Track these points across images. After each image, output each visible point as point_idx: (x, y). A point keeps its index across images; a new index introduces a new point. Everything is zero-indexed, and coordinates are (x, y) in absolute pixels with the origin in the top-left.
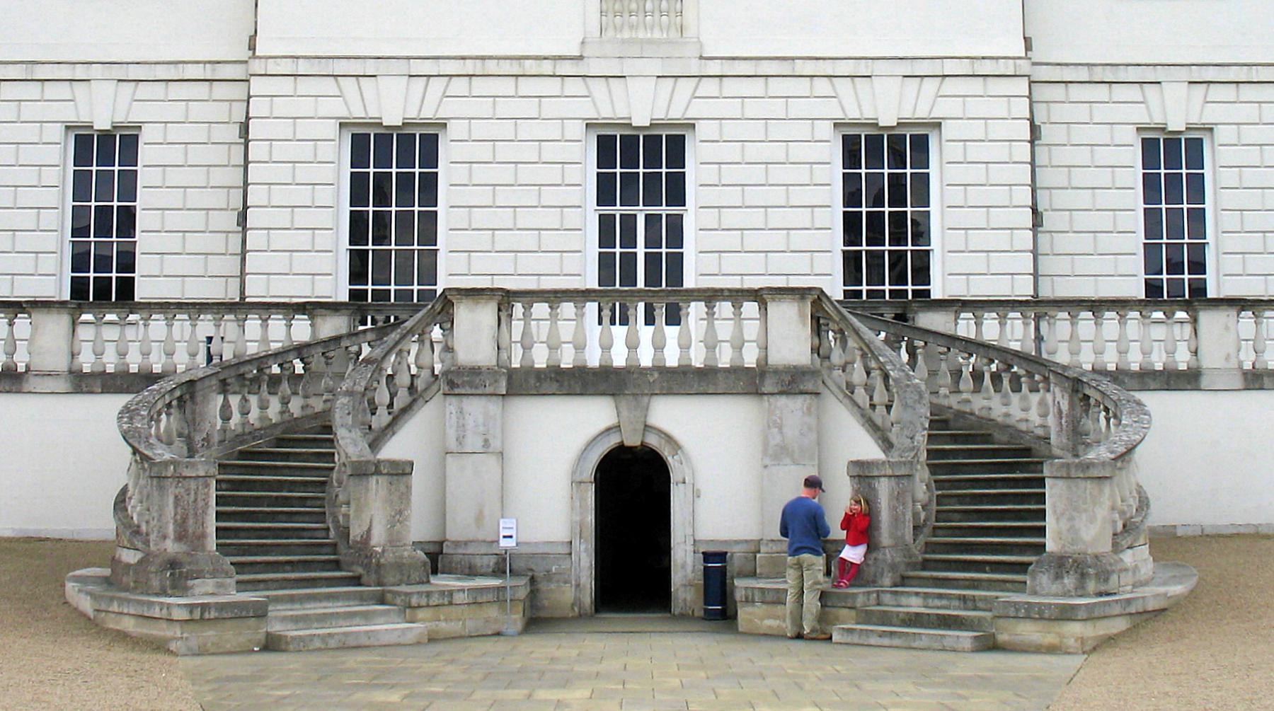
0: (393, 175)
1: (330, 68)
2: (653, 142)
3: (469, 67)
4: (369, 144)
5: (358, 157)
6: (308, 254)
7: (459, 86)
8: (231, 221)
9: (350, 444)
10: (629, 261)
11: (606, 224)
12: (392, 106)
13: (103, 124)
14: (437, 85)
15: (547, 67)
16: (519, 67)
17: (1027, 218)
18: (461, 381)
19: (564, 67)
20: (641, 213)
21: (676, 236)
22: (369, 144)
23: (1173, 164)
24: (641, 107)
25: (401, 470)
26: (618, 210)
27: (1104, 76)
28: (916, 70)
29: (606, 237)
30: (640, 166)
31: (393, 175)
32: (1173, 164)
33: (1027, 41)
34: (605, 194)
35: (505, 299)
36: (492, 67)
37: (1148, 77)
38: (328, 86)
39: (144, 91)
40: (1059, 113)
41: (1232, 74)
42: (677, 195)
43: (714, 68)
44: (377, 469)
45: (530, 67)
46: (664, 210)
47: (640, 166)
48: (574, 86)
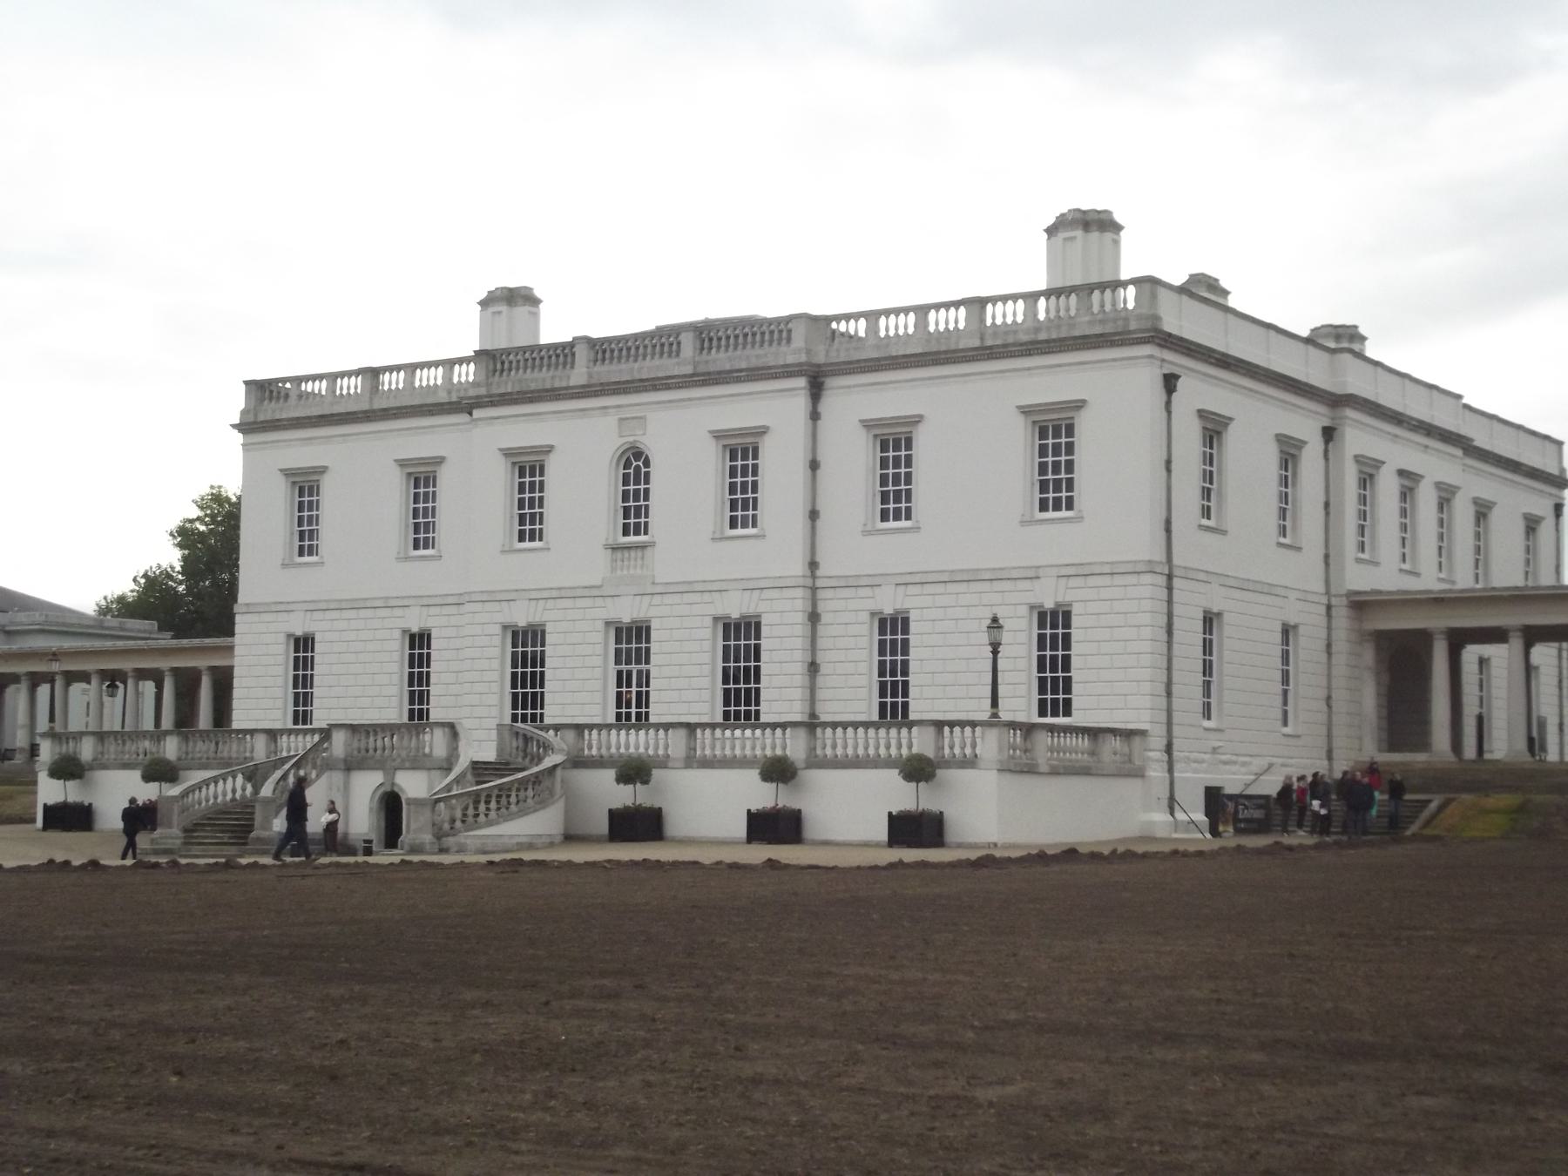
1: (492, 598)
3: (555, 594)
7: (550, 603)
11: (620, 673)
12: (522, 617)
14: (541, 603)
15: (586, 592)
19: (593, 592)
20: (634, 667)
24: (627, 612)
26: (624, 667)
27: (851, 583)
28: (751, 587)
33: (813, 565)
34: (618, 662)
36: (563, 593)
37: (874, 583)
38: (496, 606)
39: (433, 610)
40: (831, 605)
41: (917, 579)
43: (659, 589)
45: (579, 593)
46: (643, 666)
48: (599, 601)
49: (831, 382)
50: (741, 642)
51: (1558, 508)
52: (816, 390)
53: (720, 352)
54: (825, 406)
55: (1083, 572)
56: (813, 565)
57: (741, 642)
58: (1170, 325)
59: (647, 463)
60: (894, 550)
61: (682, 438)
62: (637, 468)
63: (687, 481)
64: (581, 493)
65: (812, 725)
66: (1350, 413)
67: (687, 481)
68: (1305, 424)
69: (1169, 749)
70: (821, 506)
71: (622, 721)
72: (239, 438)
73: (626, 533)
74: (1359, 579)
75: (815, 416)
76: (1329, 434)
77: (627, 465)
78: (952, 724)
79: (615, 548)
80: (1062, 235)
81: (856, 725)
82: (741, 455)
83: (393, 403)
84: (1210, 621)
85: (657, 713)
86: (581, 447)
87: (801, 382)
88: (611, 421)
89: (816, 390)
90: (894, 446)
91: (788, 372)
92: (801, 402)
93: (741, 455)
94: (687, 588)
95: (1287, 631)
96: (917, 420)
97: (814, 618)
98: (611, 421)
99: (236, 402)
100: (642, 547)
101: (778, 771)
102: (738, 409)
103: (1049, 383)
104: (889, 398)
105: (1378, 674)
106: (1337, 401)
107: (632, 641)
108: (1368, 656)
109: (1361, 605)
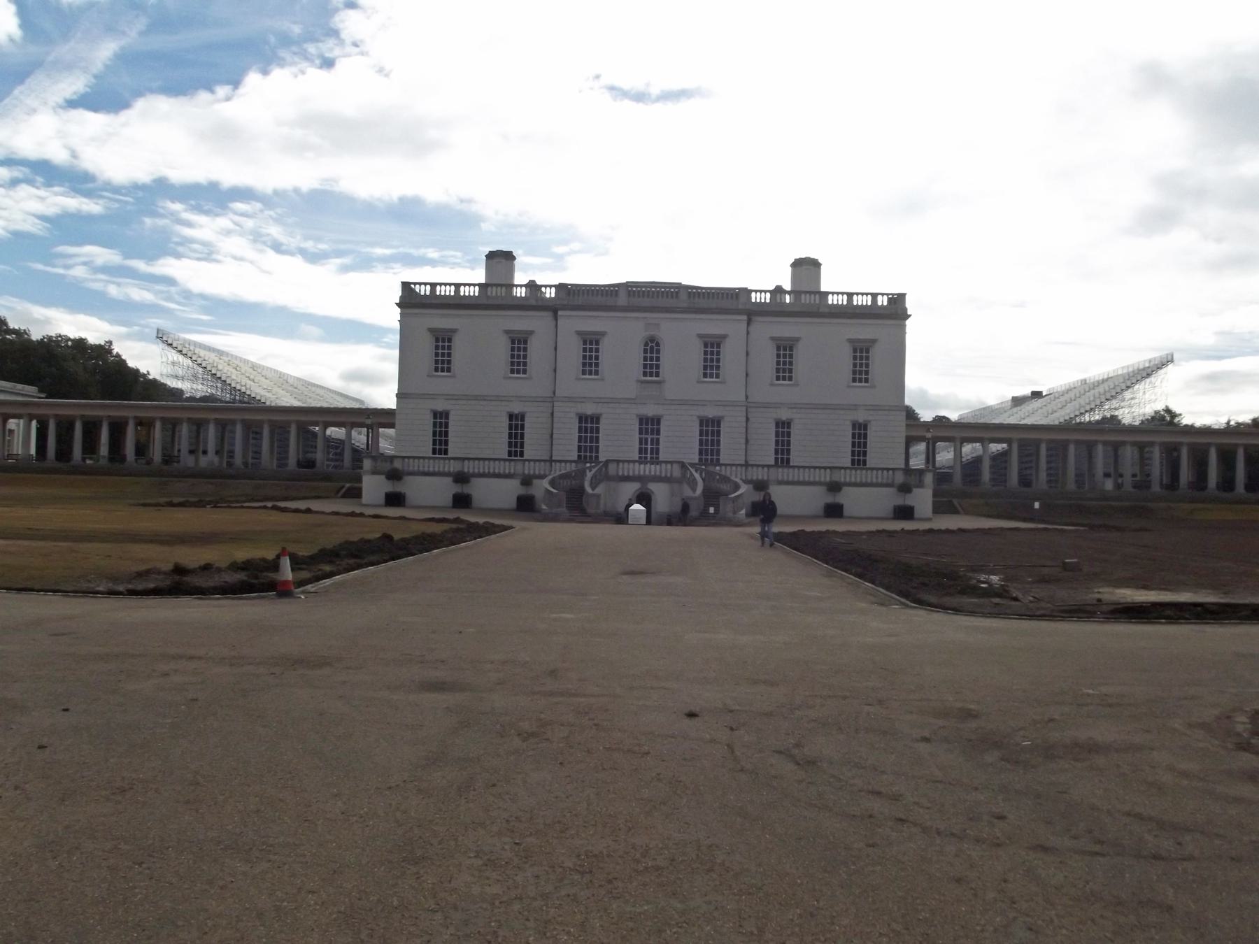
0: (589, 426)
2: (653, 420)
4: (582, 418)
5: (580, 422)
6: (567, 447)
8: (548, 437)
9: (589, 490)
10: (646, 449)
11: (641, 440)
13: (516, 412)
17: (743, 441)
18: (609, 478)
20: (649, 437)
21: (658, 443)
22: (582, 418)
23: (783, 427)
24: (650, 411)
25: (598, 496)
27: (767, 406)
29: (641, 443)
30: (650, 426)
31: (589, 426)
32: (783, 427)
33: (747, 397)
34: (640, 433)
35: (618, 462)
37: (777, 406)
42: (658, 432)
44: (593, 495)
47: (650, 426)
49: (754, 318)
50: (710, 429)
52: (749, 323)
54: (752, 329)
55: (876, 408)
57: (710, 429)
59: (658, 345)
60: (784, 392)
62: (652, 348)
63: (680, 355)
65: (747, 465)
67: (680, 355)
71: (642, 461)
72: (398, 310)
73: (645, 374)
75: (748, 333)
77: (646, 344)
78: (623, 461)
79: (643, 382)
81: (737, 465)
83: (496, 302)
85: (662, 457)
87: (745, 317)
91: (739, 312)
97: (747, 420)
99: (397, 294)
100: (659, 382)
101: (461, 478)
102: (713, 326)
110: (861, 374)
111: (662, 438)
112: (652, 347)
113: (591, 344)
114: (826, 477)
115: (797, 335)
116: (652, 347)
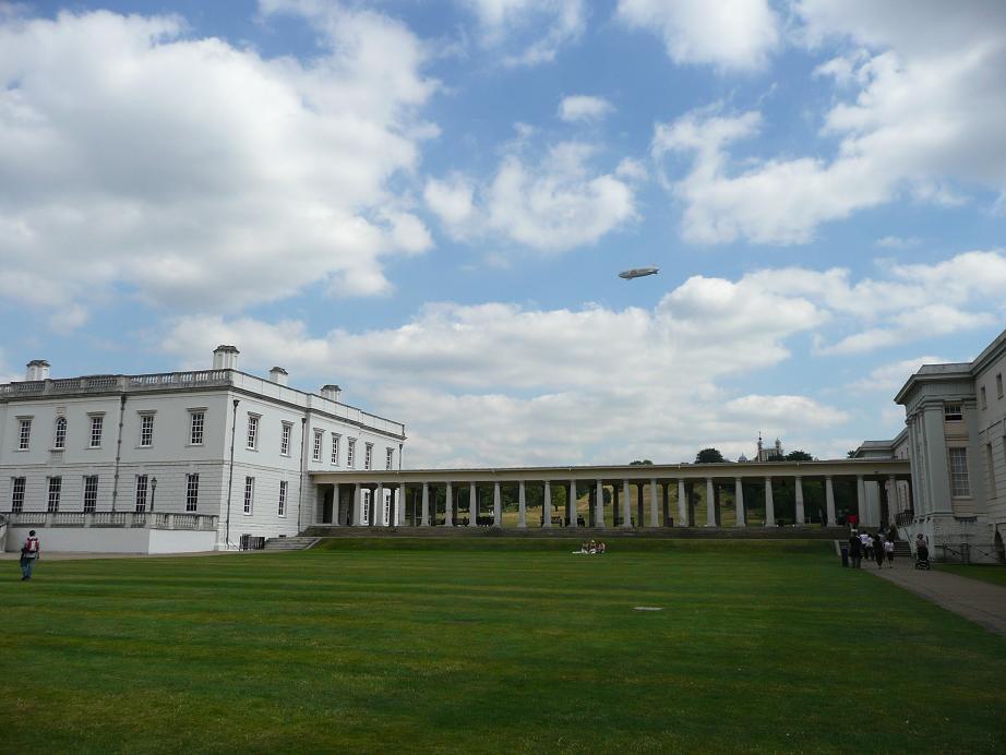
16: (37, 466)
19: (43, 466)
27: (129, 465)
33: (118, 459)
47: (55, 483)
51: (401, 446)
52: (124, 401)
53: (99, 386)
54: (126, 406)
56: (118, 459)
58: (237, 384)
61: (78, 413)
63: (79, 429)
64: (43, 433)
65: (113, 512)
66: (312, 414)
67: (79, 429)
68: (295, 418)
69: (228, 522)
70: (122, 439)
74: (313, 467)
75: (123, 409)
76: (304, 420)
79: (52, 451)
80: (218, 354)
82: (97, 420)
84: (249, 480)
86: (44, 416)
87: (120, 398)
88: (54, 408)
89: (124, 401)
90: (148, 418)
92: (119, 404)
93: (97, 420)
94: (75, 466)
95: (283, 484)
96: (154, 412)
97: (117, 477)
98: (54, 408)
102: (96, 405)
103: (197, 401)
104: (147, 404)
105: (318, 497)
106: (308, 410)
107: (55, 483)
108: (315, 492)
109: (312, 476)
110: (197, 435)
111: (61, 493)
112: (62, 423)
113: (26, 423)
114: (60, 519)
115: (30, 414)
116: (62, 423)
